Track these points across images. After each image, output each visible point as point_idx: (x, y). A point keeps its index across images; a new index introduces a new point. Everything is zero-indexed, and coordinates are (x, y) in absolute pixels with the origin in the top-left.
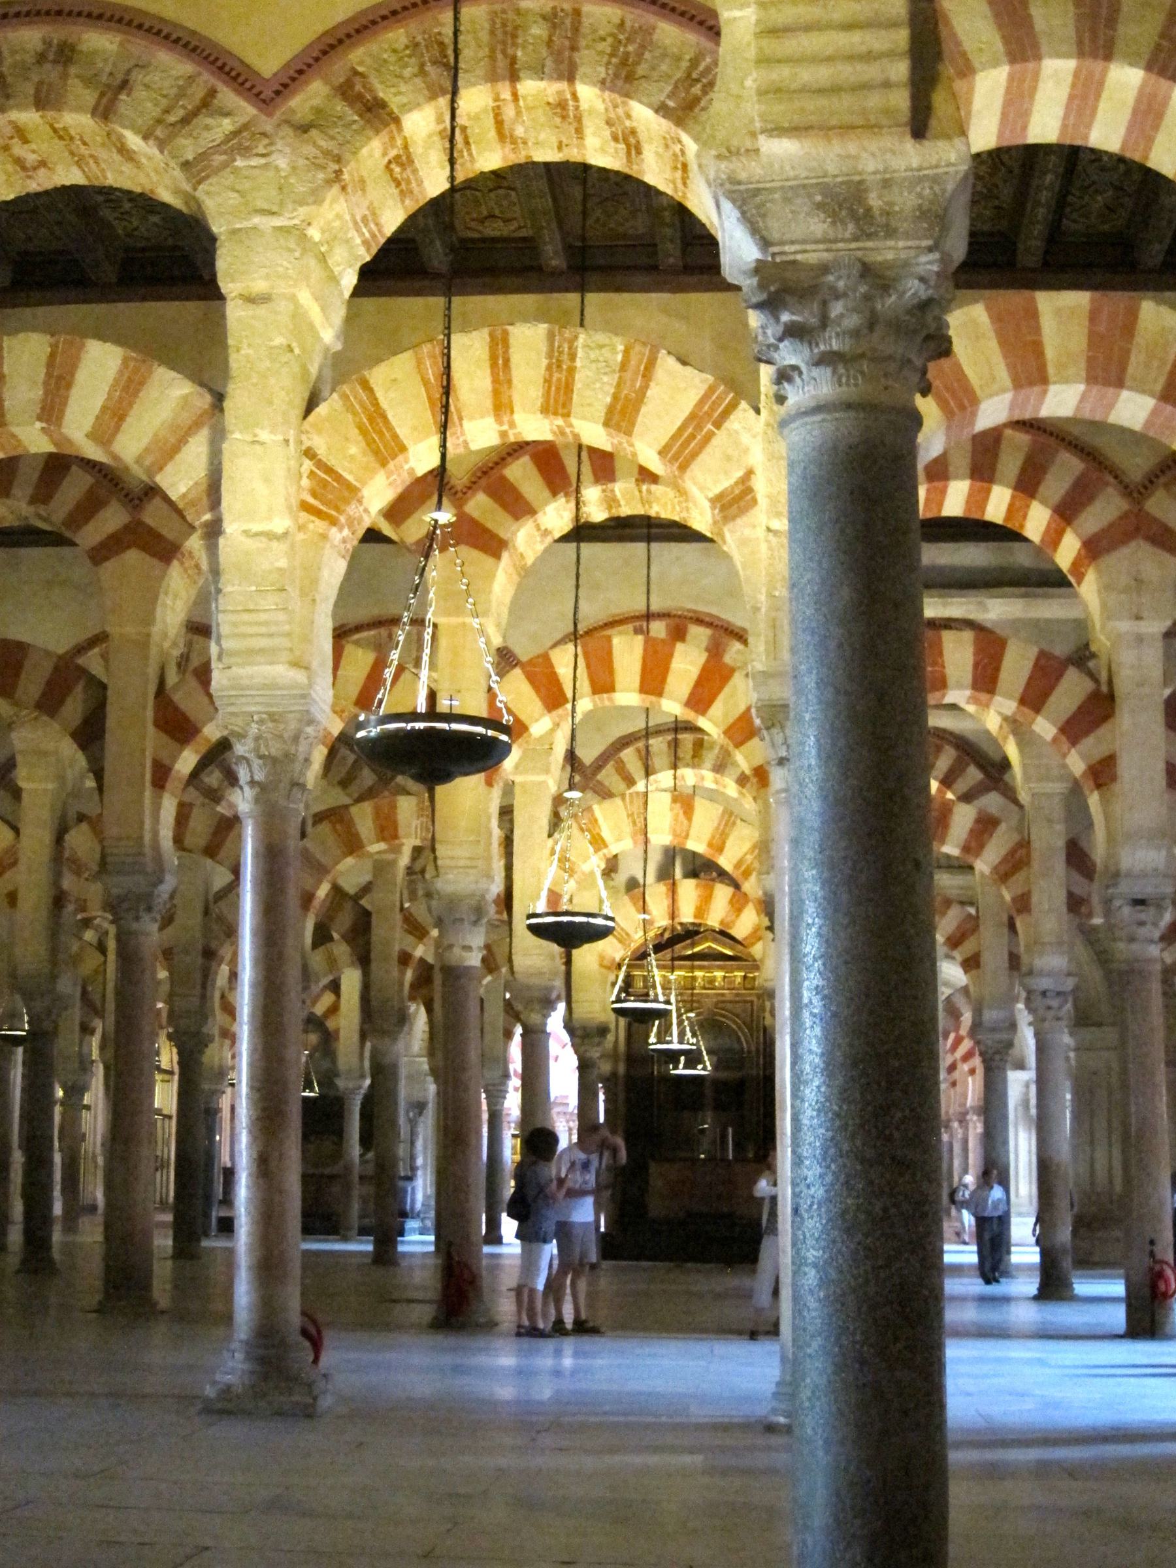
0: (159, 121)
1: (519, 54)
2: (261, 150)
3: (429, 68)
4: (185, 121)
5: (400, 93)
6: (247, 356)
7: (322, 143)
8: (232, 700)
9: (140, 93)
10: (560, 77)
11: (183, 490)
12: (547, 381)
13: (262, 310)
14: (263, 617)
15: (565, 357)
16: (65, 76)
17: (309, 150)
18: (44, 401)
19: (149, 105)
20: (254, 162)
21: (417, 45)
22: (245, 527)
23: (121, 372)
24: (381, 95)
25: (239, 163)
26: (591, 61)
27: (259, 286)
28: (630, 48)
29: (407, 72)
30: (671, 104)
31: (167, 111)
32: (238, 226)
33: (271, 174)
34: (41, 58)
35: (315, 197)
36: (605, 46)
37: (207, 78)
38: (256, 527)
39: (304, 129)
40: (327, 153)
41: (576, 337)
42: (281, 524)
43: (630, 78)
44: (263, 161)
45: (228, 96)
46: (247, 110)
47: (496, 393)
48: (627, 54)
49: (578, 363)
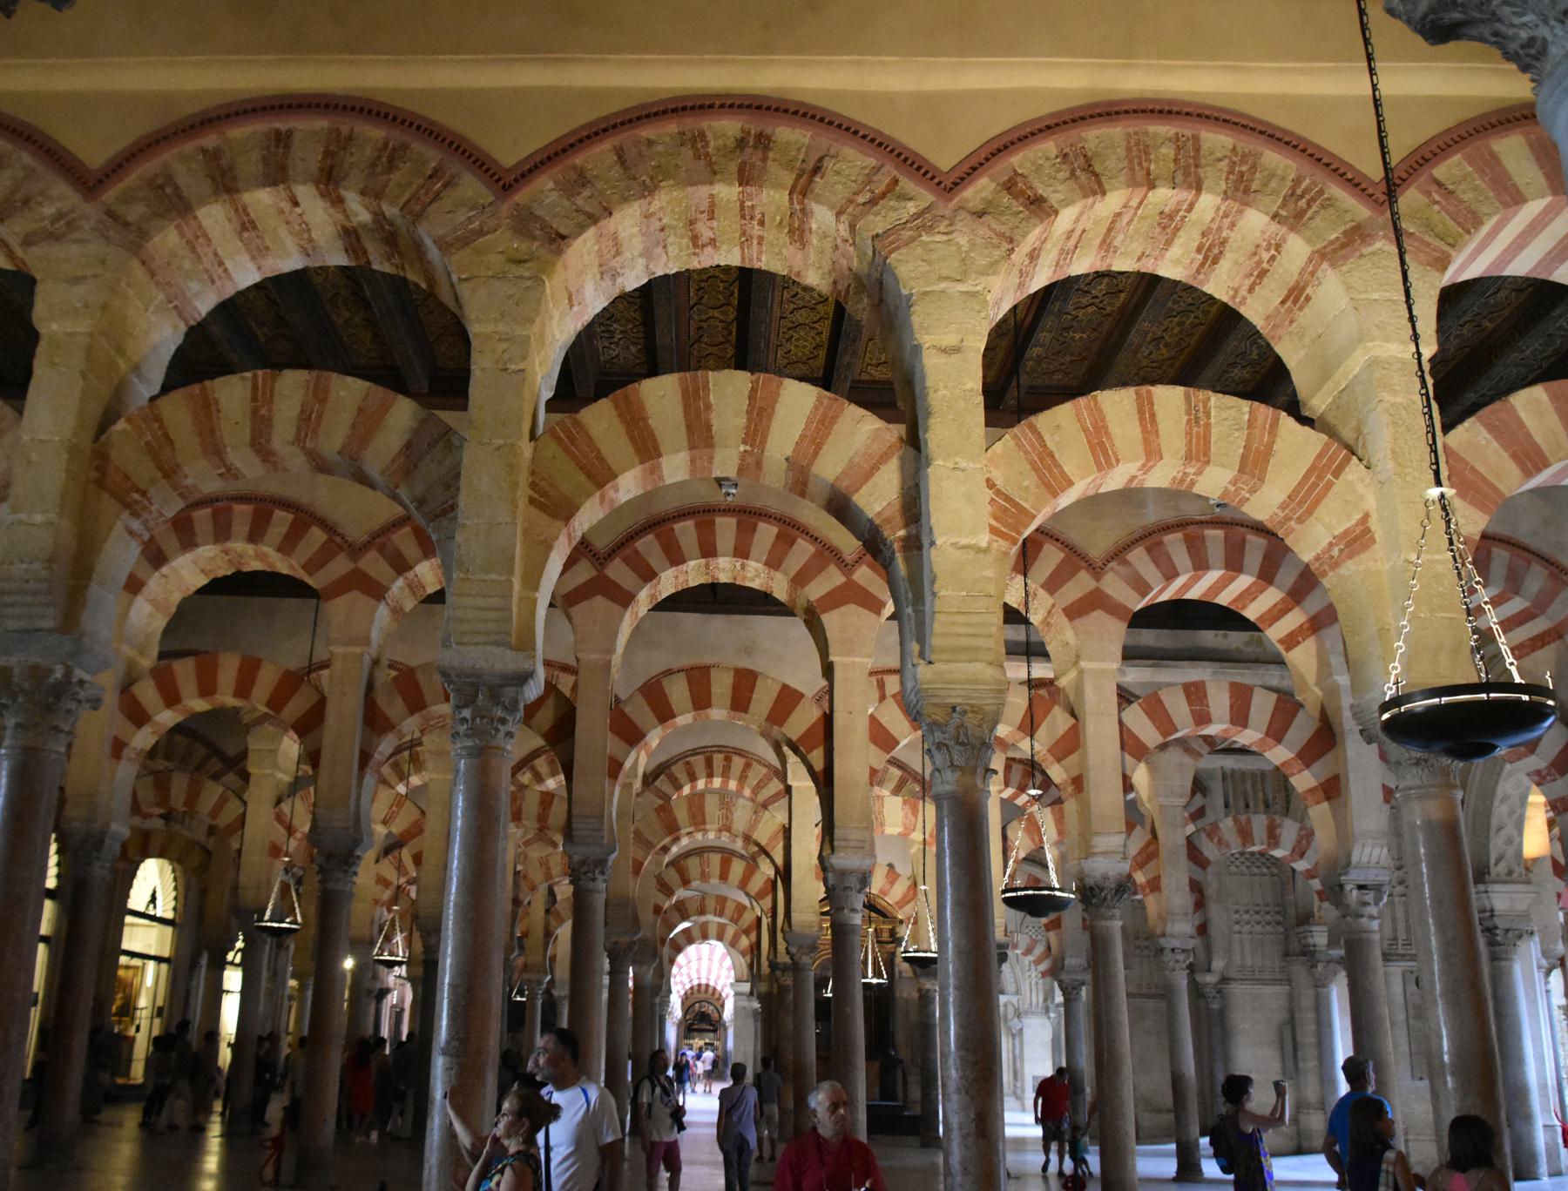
0: (851, 201)
1: (1152, 167)
2: (942, 228)
3: (1078, 172)
4: (873, 202)
5: (1057, 192)
6: (944, 396)
7: (994, 226)
8: (936, 693)
9: (830, 177)
10: (1189, 187)
11: (878, 509)
12: (1189, 433)
13: (955, 358)
14: (976, 619)
15: (1201, 415)
16: (764, 160)
17: (983, 231)
18: (748, 427)
19: (841, 187)
20: (938, 238)
21: (1066, 155)
22: (953, 540)
23: (816, 407)
24: (1040, 192)
25: (925, 238)
26: (1215, 177)
27: (951, 339)
28: (1244, 168)
29: (1061, 175)
30: (1283, 213)
31: (856, 194)
32: (928, 289)
33: (953, 248)
34: (741, 143)
35: (992, 268)
36: (1224, 164)
37: (890, 170)
38: (965, 541)
39: (980, 214)
40: (1001, 235)
41: (1209, 399)
42: (984, 539)
43: (1247, 191)
44: (945, 238)
45: (907, 184)
46: (924, 197)
47: (1146, 442)
48: (1242, 174)
49: (1213, 420)
